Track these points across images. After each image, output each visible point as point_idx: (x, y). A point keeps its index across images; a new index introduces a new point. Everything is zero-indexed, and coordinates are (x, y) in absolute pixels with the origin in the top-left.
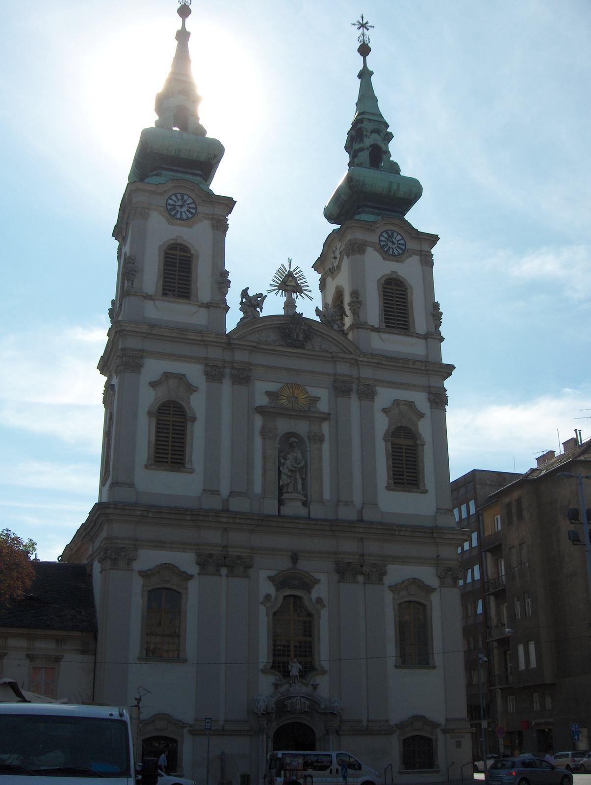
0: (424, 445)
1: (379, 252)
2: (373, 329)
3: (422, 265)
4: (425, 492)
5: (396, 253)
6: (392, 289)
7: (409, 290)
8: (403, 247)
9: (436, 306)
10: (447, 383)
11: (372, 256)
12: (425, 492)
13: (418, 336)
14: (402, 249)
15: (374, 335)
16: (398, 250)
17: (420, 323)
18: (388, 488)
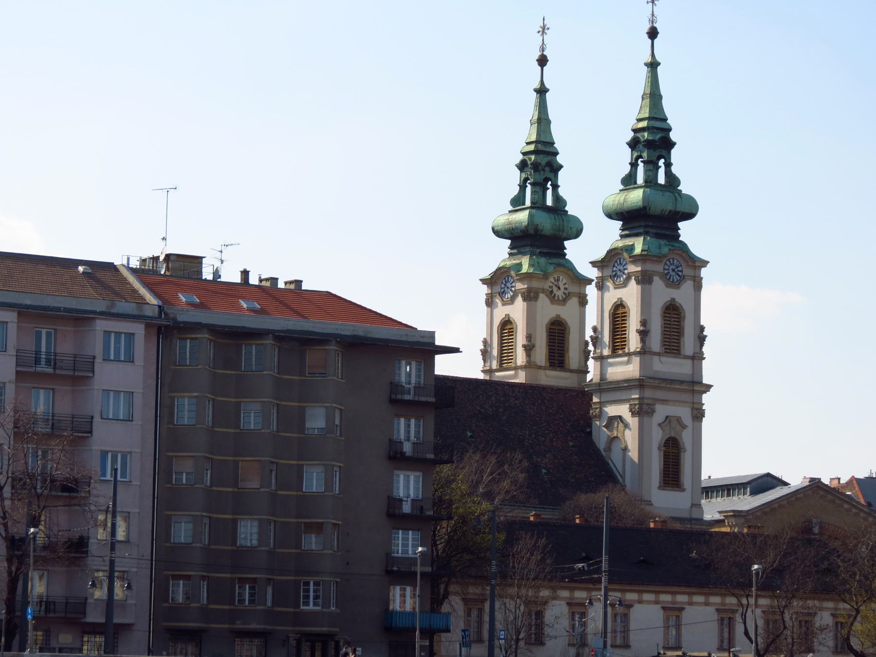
0: (685, 452)
1: (664, 281)
2: (655, 354)
3: (695, 291)
4: (684, 490)
5: (675, 281)
6: (670, 314)
7: (683, 315)
8: (680, 273)
9: (702, 329)
10: (705, 398)
11: (658, 283)
12: (684, 490)
13: (687, 357)
14: (679, 276)
15: (656, 359)
16: (677, 277)
17: (688, 345)
18: (659, 488)
